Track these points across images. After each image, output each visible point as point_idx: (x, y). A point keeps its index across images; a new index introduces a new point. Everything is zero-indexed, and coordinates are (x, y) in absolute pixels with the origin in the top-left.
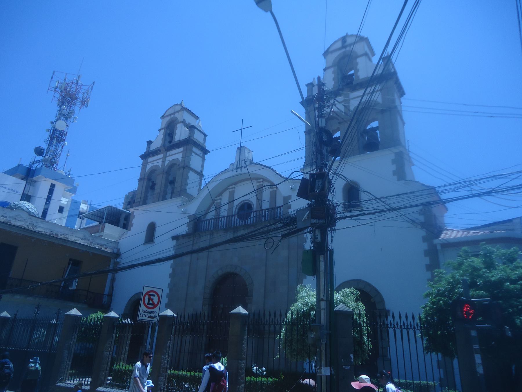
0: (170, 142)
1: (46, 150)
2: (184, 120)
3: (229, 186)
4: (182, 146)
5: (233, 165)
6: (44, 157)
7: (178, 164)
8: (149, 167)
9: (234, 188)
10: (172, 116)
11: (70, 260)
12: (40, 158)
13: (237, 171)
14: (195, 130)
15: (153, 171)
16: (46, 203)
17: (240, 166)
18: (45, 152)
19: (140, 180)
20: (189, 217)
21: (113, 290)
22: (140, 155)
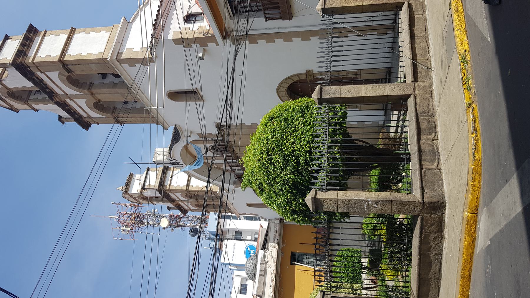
10: (137, 199)
13: (182, 165)
14: (147, 183)
16: (239, 220)
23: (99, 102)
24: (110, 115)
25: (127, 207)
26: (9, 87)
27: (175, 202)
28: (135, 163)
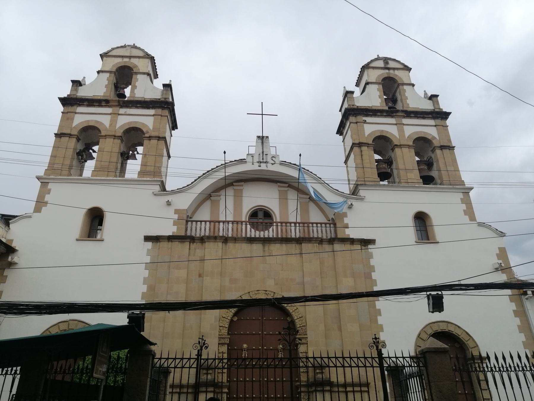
3: (235, 182)
4: (153, 108)
5: (253, 157)
7: (145, 130)
9: (242, 186)
10: (126, 60)
17: (265, 161)
19: (58, 135)
20: (177, 211)
22: (62, 96)
24: (370, 142)
27: (118, 105)
28: (262, 114)
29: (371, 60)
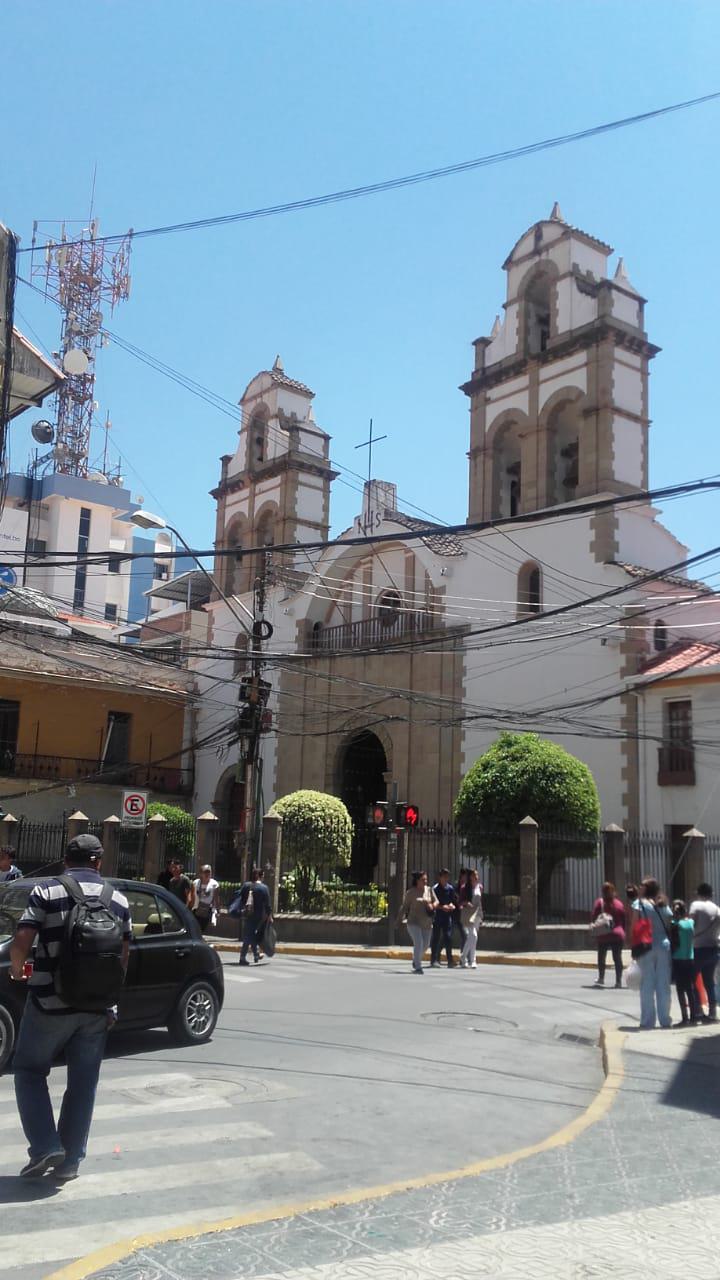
0: (261, 459)
1: (55, 427)
2: (281, 410)
6: (56, 444)
8: (229, 513)
9: (371, 562)
10: (259, 400)
11: (111, 713)
12: (46, 449)
13: (365, 534)
14: (302, 434)
15: (236, 525)
18: (55, 432)
20: (298, 623)
21: (194, 761)
23: (521, 436)
24: (490, 440)
25: (114, 262)
26: (559, 284)
29: (517, 244)
